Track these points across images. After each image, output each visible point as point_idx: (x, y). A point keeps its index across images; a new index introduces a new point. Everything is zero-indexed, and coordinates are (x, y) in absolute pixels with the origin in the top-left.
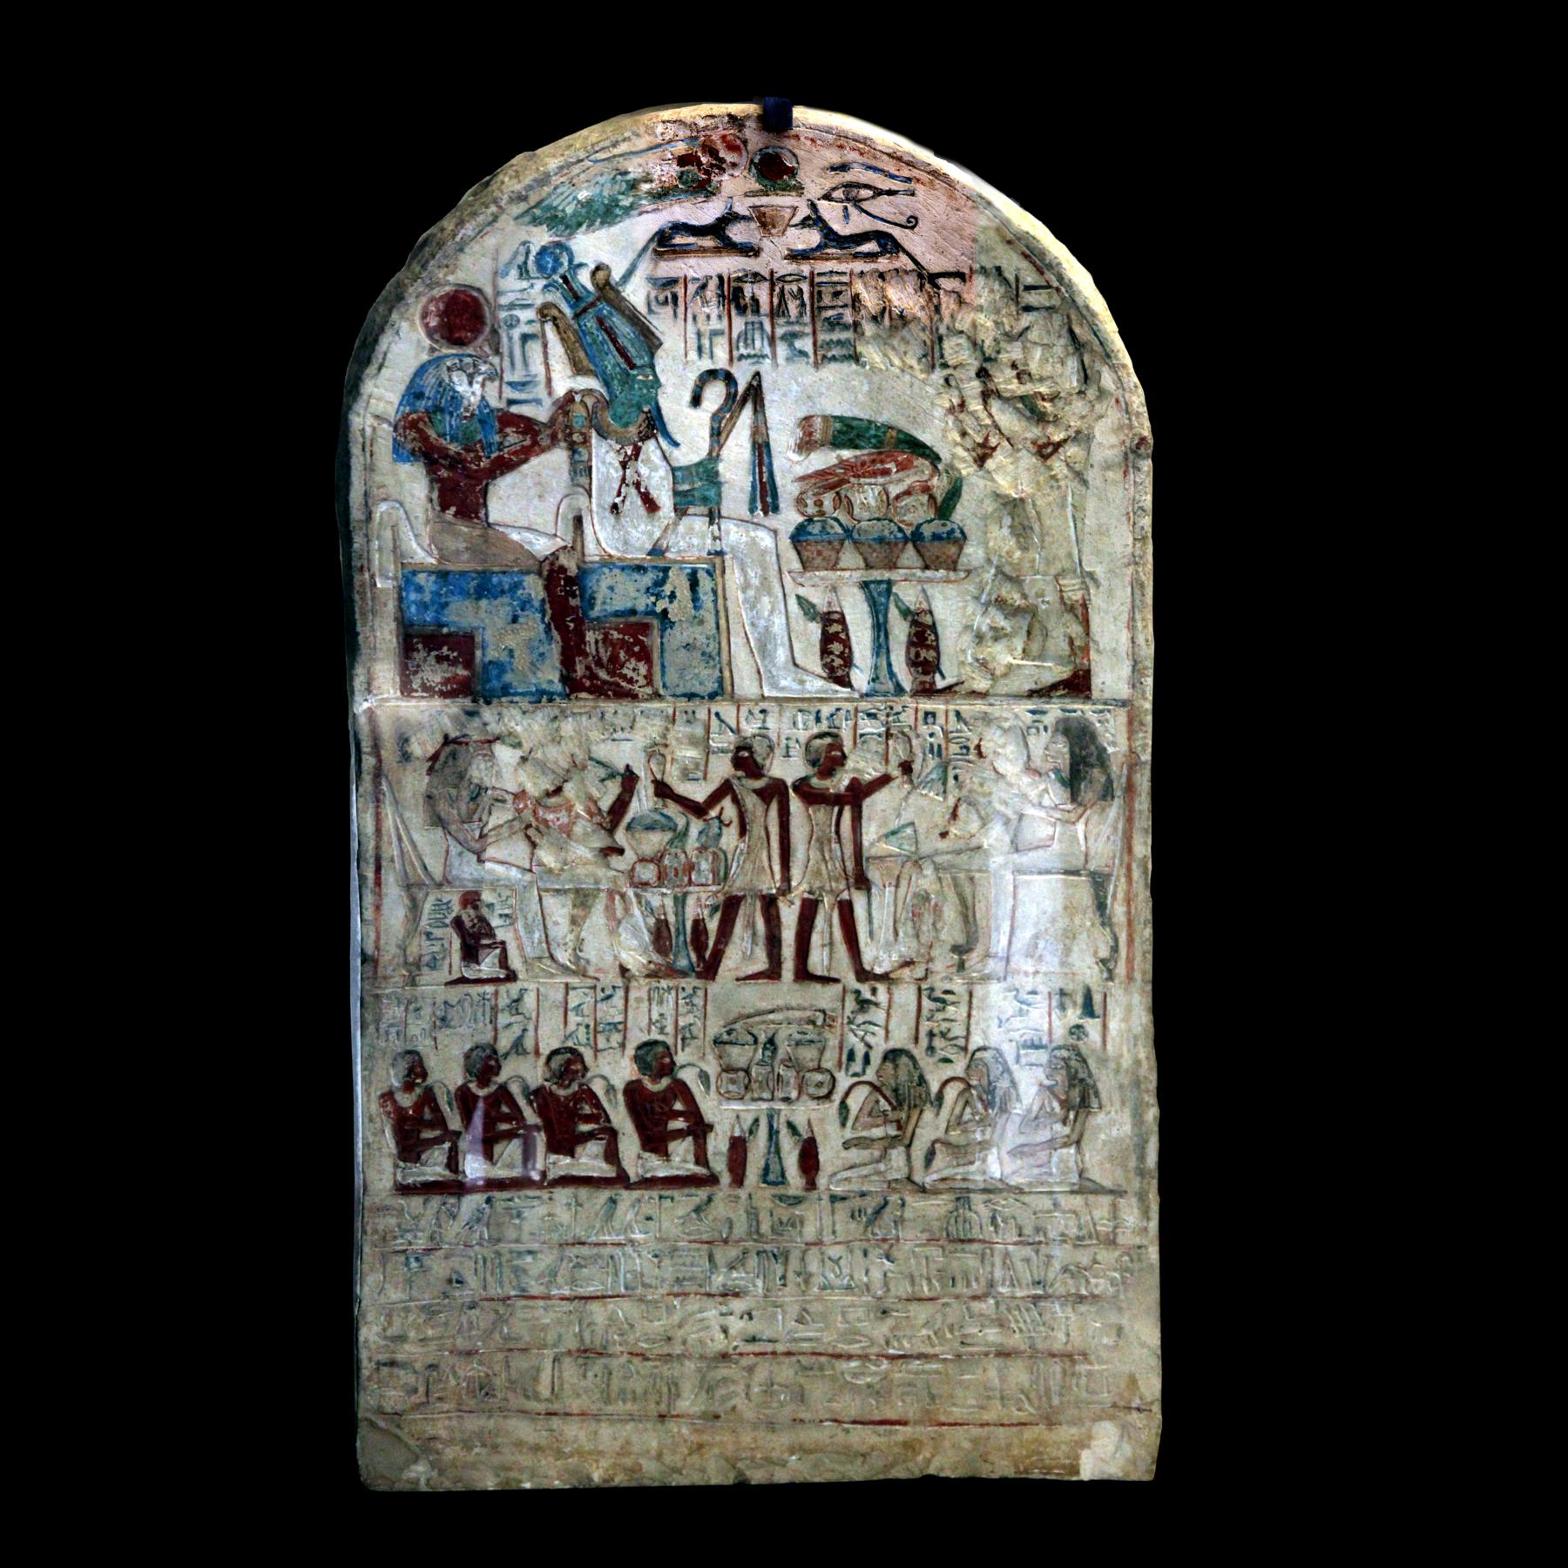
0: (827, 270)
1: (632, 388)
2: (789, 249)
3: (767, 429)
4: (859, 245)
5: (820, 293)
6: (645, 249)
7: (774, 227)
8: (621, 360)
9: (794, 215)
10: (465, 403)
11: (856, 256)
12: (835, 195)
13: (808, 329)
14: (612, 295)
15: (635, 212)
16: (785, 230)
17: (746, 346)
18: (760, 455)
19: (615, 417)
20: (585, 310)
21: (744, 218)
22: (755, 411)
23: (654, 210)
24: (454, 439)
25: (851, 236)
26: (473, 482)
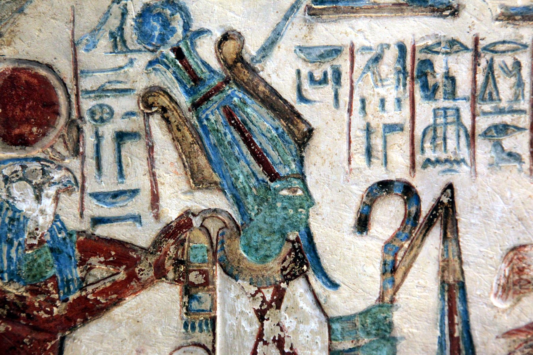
1: (273, 207)
2: (502, 6)
3: (461, 262)
8: (258, 169)
10: (31, 226)
14: (245, 75)
17: (435, 148)
18: (451, 300)
19: (248, 248)
20: (206, 98)
22: (445, 237)
24: (14, 277)
26: (41, 336)
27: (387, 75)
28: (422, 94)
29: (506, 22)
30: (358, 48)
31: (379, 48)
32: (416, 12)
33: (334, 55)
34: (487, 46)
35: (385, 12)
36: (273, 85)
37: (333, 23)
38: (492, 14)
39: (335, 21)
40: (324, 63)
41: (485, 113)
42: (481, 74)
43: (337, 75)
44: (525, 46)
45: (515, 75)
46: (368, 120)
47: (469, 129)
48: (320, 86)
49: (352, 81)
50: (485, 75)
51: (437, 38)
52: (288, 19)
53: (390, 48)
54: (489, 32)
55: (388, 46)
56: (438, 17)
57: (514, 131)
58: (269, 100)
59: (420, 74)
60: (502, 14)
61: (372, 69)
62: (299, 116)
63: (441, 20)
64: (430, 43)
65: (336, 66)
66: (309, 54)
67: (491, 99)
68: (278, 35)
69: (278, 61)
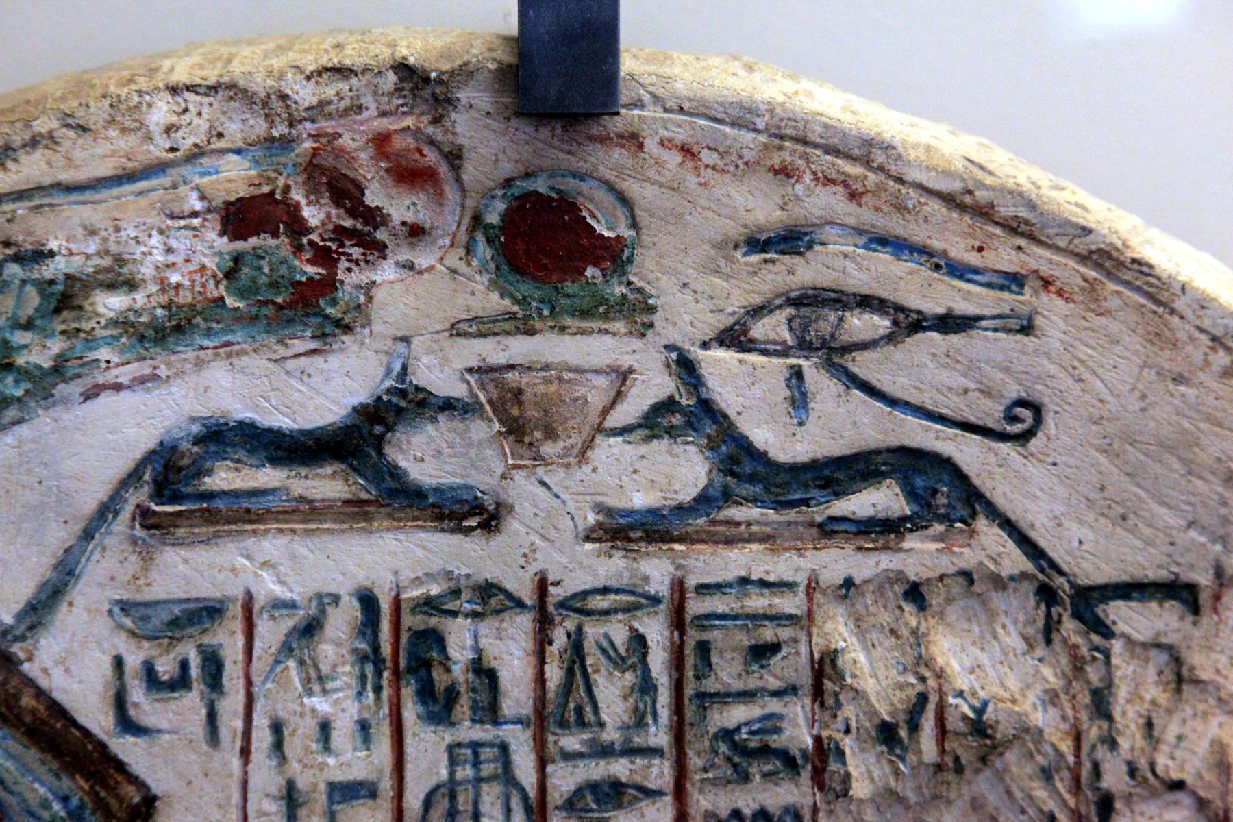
0: (731, 575)
2: (600, 508)
4: (838, 495)
5: (704, 649)
6: (106, 511)
7: (551, 434)
9: (618, 396)
11: (829, 530)
12: (761, 329)
13: (660, 773)
15: (74, 389)
16: (588, 445)
21: (448, 405)
23: (141, 381)
25: (813, 466)
27: (335, 666)
28: (420, 709)
29: (609, 544)
30: (262, 603)
31: (314, 603)
32: (400, 520)
33: (205, 620)
34: (567, 599)
35: (325, 521)
36: (58, 696)
37: (202, 546)
38: (576, 527)
39: (207, 542)
40: (179, 640)
41: (568, 756)
42: (555, 664)
43: (213, 665)
44: (655, 600)
45: (633, 667)
46: (290, 774)
47: (532, 793)
48: (171, 695)
49: (249, 683)
50: (565, 666)
51: (450, 580)
52: (93, 538)
53: (341, 604)
54: (570, 567)
55: (336, 599)
56: (452, 531)
57: (636, 798)
58: (46, 728)
59: (413, 664)
60: (600, 525)
61: (297, 652)
62: (120, 767)
63: (457, 539)
64: (435, 590)
65: (211, 646)
66: (145, 619)
67: (582, 723)
68: (69, 574)
69: (68, 636)
